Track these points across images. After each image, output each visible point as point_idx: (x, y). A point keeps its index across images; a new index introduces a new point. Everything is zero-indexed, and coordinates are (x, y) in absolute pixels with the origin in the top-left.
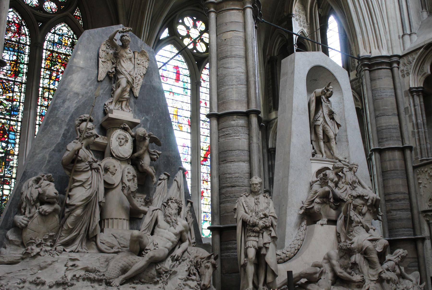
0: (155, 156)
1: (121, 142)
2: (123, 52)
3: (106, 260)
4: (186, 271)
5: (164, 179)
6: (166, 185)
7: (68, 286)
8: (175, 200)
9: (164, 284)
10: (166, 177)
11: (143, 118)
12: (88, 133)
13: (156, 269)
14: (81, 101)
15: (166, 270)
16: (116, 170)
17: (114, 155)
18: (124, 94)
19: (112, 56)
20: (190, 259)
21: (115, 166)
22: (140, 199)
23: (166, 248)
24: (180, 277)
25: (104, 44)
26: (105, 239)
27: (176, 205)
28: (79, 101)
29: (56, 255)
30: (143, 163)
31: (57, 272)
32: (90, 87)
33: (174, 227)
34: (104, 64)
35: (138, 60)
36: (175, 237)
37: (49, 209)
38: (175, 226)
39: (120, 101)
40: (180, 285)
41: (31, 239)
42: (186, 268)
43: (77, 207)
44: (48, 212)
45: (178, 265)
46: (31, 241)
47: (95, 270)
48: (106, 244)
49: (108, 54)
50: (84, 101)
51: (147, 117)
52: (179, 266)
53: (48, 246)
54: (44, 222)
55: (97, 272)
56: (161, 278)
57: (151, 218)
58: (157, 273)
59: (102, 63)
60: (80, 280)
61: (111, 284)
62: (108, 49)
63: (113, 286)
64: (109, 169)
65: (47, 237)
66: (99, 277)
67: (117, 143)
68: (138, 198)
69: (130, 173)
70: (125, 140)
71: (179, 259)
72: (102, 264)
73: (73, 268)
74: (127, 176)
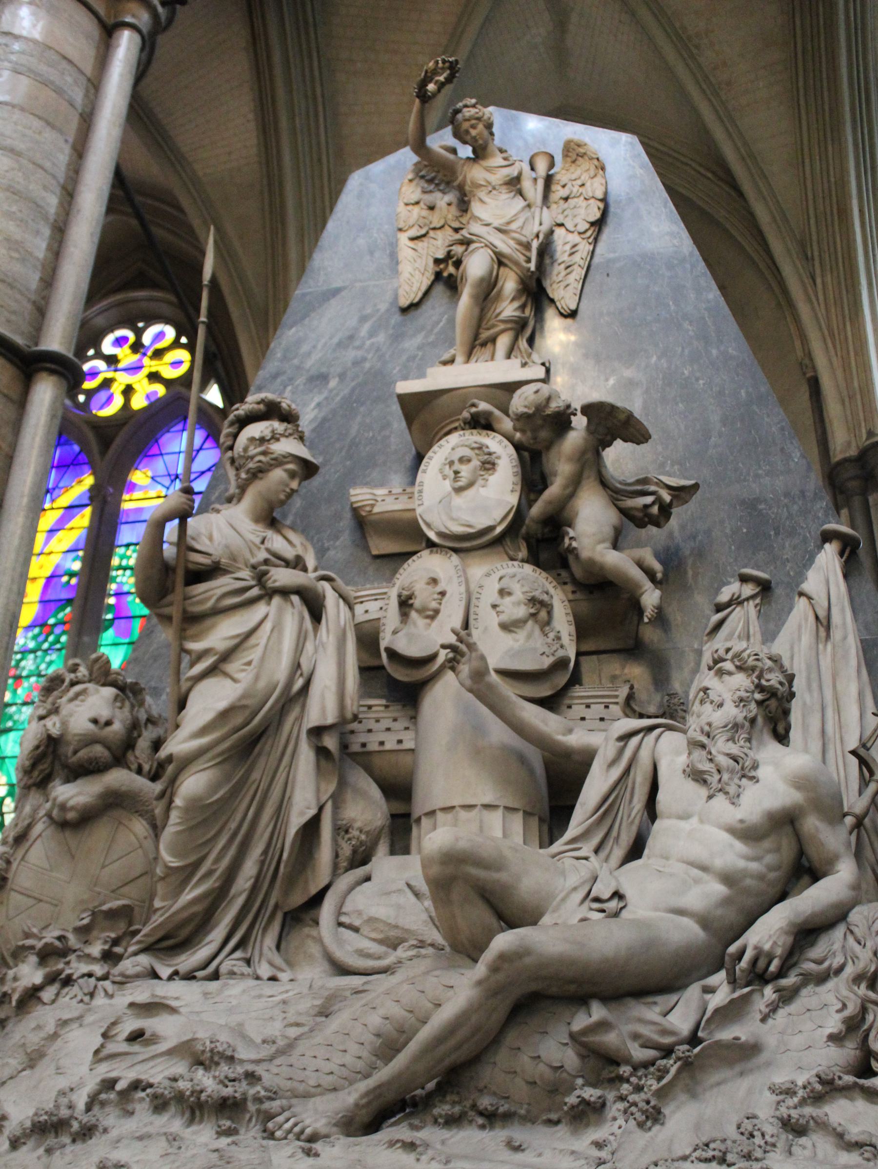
0: (649, 499)
1: (456, 473)
2: (477, 174)
3: (323, 1006)
4: (835, 1039)
5: (736, 601)
6: (755, 627)
7: (74, 1141)
8: (732, 660)
9: (632, 1123)
10: (748, 590)
11: (612, 382)
12: (252, 458)
13: (572, 1036)
14: (337, 394)
15: (667, 1040)
16: (443, 594)
17: (432, 536)
18: (498, 311)
19: (454, 211)
20: (861, 965)
21: (434, 581)
22: (597, 710)
23: (681, 912)
24: (780, 1078)
25: (411, 181)
26: (361, 907)
27: (741, 681)
28: (326, 398)
29: (102, 994)
30: (571, 538)
31: (59, 1071)
32: (373, 340)
33: (727, 793)
34: (419, 245)
35: (564, 186)
36: (739, 846)
38: (732, 789)
39: (484, 345)
40: (748, 1125)
41: (27, 935)
42: (834, 1023)
43: (187, 762)
44: (72, 808)
45: (774, 1008)
46: (20, 943)
47: (212, 1051)
48: (365, 930)
49: (432, 208)
50: (346, 391)
51: (628, 373)
52: (782, 1013)
53: (89, 958)
54: (73, 857)
55: (217, 1064)
56: (625, 1088)
57: (616, 772)
58: (582, 1057)
59: (411, 244)
60: (138, 1107)
61: (270, 1125)
62: (431, 192)
63: (278, 1134)
64: (410, 597)
65: (85, 922)
66: (220, 1086)
67: (447, 485)
68: (588, 706)
69: (510, 594)
70: (476, 463)
71: (773, 968)
72: (298, 1025)
73: (136, 1048)
74: (494, 606)
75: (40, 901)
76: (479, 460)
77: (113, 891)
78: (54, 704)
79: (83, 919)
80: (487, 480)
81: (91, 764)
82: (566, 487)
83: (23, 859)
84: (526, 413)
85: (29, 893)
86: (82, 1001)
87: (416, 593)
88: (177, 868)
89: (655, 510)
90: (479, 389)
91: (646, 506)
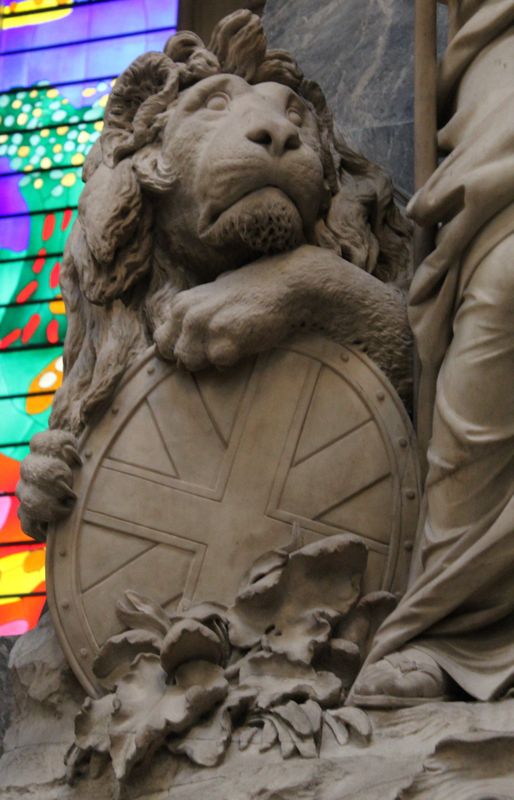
29: (342, 736)
37: (236, 300)
46: (117, 639)
65: (269, 581)
75: (156, 543)
77: (318, 518)
78: (149, 123)
79: (261, 576)
81: (257, 234)
83: (106, 455)
85: (129, 528)
86: (296, 753)
88: (487, 445)
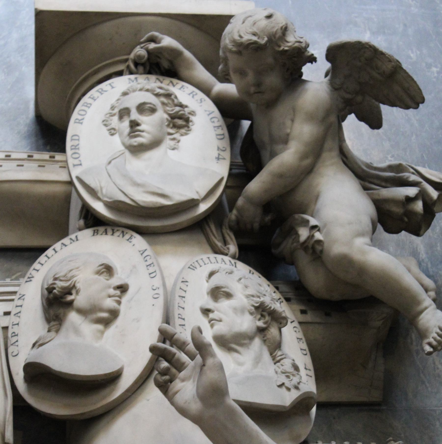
0: (412, 191)
76: (166, 112)
80: (179, 141)
82: (304, 156)
84: (255, 43)
87: (78, 285)
89: (419, 206)
90: (159, 19)
91: (409, 200)
